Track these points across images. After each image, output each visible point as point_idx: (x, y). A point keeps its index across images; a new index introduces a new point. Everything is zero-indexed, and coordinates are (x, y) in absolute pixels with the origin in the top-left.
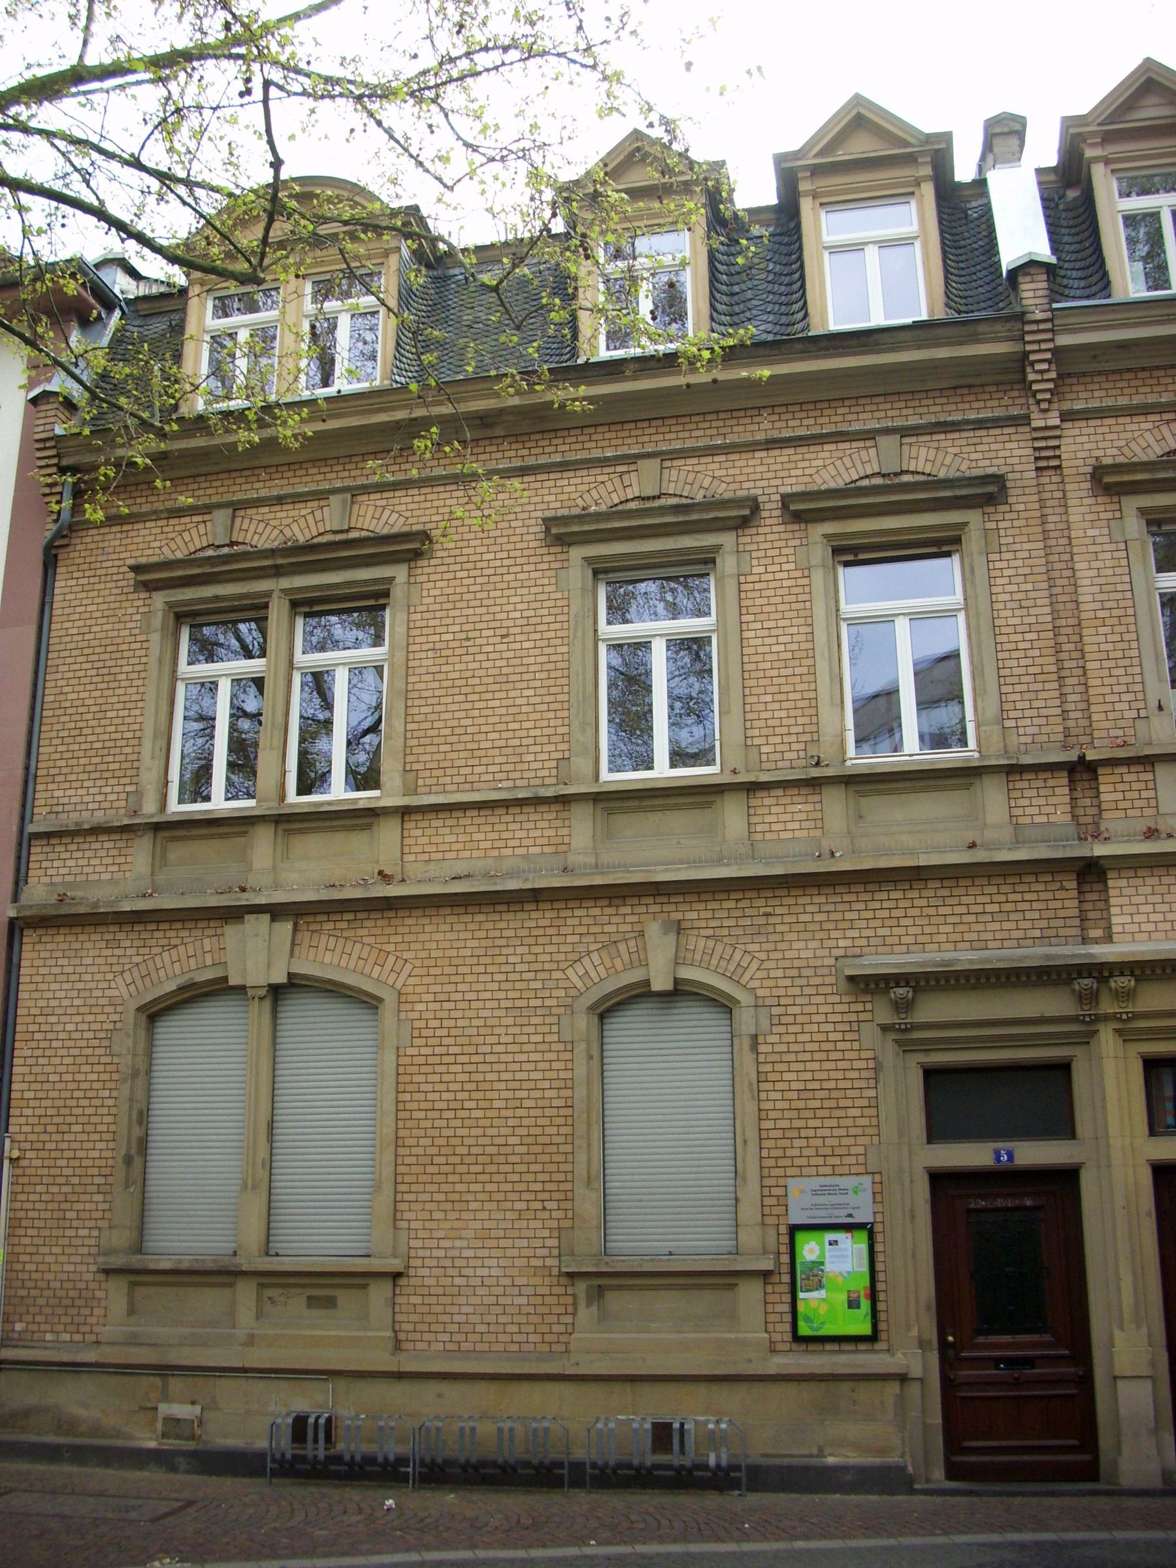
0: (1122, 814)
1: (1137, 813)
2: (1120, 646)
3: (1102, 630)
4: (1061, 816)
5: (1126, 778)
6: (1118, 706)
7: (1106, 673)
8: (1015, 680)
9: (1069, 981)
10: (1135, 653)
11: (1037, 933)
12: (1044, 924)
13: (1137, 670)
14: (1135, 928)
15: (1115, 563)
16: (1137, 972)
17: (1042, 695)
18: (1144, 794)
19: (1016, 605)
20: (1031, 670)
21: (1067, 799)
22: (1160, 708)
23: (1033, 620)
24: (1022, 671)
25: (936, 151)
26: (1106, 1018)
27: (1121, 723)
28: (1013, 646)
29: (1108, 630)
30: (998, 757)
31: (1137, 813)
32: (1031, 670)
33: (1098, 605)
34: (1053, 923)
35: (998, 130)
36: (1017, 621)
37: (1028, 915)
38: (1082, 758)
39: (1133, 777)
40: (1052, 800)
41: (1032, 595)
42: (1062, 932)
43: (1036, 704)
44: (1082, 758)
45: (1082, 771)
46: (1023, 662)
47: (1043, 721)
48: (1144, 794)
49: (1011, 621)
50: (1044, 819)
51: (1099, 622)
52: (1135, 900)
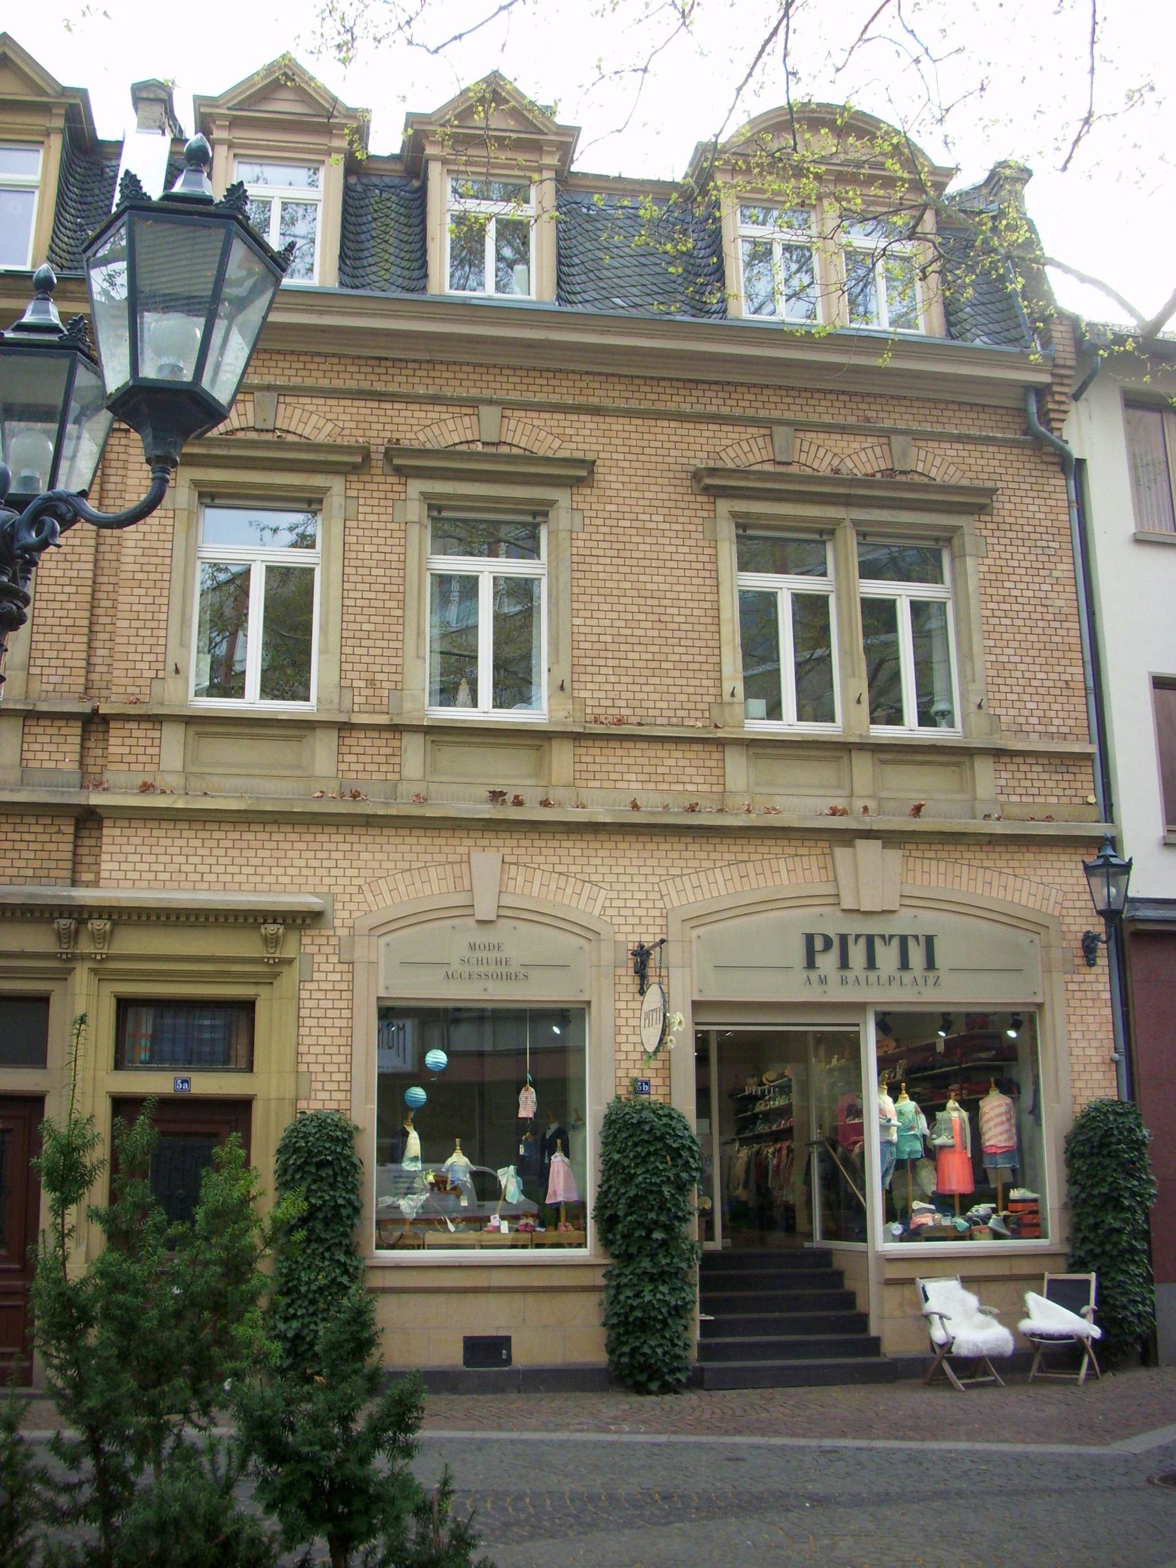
0: (126, 767)
1: (140, 767)
2: (150, 608)
3: (136, 591)
4: (70, 764)
5: (136, 733)
6: (139, 665)
7: (133, 632)
8: (48, 629)
9: (51, 920)
10: (163, 616)
11: (30, 872)
12: (38, 864)
13: (163, 633)
14: (121, 875)
15: (161, 529)
16: (115, 917)
17: (70, 647)
18: (150, 751)
19: (61, 558)
20: (64, 622)
21: (78, 748)
22: (177, 671)
23: (74, 574)
24: (56, 621)
25: (71, 105)
26: (83, 957)
27: (139, 682)
28: (51, 597)
29: (142, 591)
30: (16, 701)
31: (140, 767)
32: (64, 622)
33: (137, 568)
34: (46, 864)
35: (145, 95)
36: (59, 573)
37: (24, 855)
38: (95, 711)
39: (141, 733)
40: (63, 748)
41: (77, 550)
42: (53, 873)
43: (62, 655)
44: (95, 711)
45: (94, 723)
46: (58, 613)
47: (67, 672)
48: (150, 751)
49: (55, 573)
50: (52, 765)
51: (136, 583)
52: (126, 849)
